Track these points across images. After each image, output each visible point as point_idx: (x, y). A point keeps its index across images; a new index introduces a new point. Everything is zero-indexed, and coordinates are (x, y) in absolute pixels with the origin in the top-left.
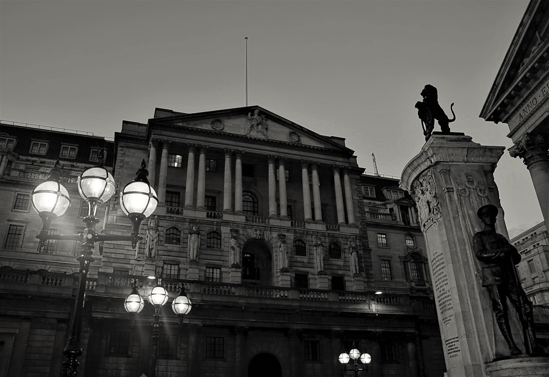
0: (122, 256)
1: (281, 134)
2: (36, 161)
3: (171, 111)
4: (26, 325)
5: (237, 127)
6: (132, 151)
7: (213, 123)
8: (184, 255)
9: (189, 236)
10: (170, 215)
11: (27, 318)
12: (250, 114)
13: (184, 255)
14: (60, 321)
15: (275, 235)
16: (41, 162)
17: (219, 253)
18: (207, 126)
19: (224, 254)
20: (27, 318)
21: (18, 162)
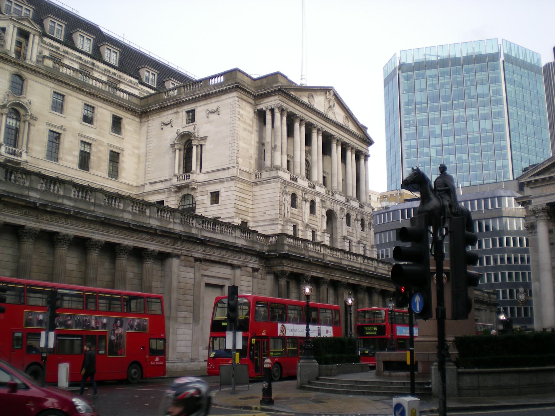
0: (244, 209)
1: (339, 116)
2: (58, 48)
3: (286, 77)
4: (238, 272)
5: (319, 102)
6: (244, 103)
7: (308, 98)
8: (300, 218)
9: (304, 202)
10: (291, 181)
11: (239, 267)
12: (328, 93)
13: (300, 218)
14: (255, 270)
15: (338, 207)
16: (64, 52)
17: (315, 219)
18: (305, 100)
19: (318, 220)
20: (239, 267)
21: (43, 45)
